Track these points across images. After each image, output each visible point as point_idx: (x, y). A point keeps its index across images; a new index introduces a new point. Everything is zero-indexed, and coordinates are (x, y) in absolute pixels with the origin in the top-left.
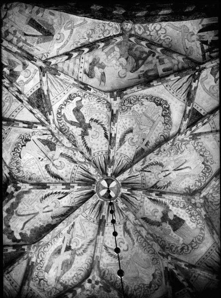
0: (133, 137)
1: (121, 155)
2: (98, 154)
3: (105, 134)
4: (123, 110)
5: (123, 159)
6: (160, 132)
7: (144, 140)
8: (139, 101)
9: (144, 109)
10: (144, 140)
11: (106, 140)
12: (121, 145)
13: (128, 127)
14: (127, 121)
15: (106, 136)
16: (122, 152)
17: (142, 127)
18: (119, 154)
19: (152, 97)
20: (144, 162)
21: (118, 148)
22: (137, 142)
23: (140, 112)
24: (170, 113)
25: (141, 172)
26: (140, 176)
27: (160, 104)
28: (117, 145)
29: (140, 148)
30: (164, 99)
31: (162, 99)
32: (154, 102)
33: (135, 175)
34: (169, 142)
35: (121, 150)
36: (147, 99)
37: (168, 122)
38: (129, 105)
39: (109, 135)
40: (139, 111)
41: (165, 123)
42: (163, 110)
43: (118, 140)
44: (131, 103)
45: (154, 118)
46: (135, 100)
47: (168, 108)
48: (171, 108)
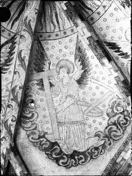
0: (71, 75)
1: (65, 33)
2: (104, 7)
3: (119, 48)
4: (119, 105)
5: (57, 29)
6: (39, 119)
7: (51, 85)
8: (106, 136)
9: (88, 130)
10: (51, 85)
11: (108, 39)
12: (79, 49)
13: (90, 84)
14: (98, 92)
15: (113, 46)
16: (67, 39)
17: (70, 101)
18: (69, 32)
19: (92, 158)
20: (22, 60)
21: (78, 42)
22: (59, 73)
23: (90, 121)
24: (49, 156)
25: (12, 35)
26: (9, 28)
27: (72, 156)
28: (85, 44)
29: (46, 68)
30: (73, 168)
31: (76, 165)
32: (83, 153)
33: (17, 23)
34: (15, 123)
35: (71, 41)
36: (97, 149)
37: (41, 142)
38: (116, 118)
39: (112, 52)
40: (94, 121)
41: (44, 137)
42: (61, 151)
43: (90, 53)
44: (114, 124)
45: (63, 129)
46: (112, 133)
47: (57, 161)
48: (54, 164)
